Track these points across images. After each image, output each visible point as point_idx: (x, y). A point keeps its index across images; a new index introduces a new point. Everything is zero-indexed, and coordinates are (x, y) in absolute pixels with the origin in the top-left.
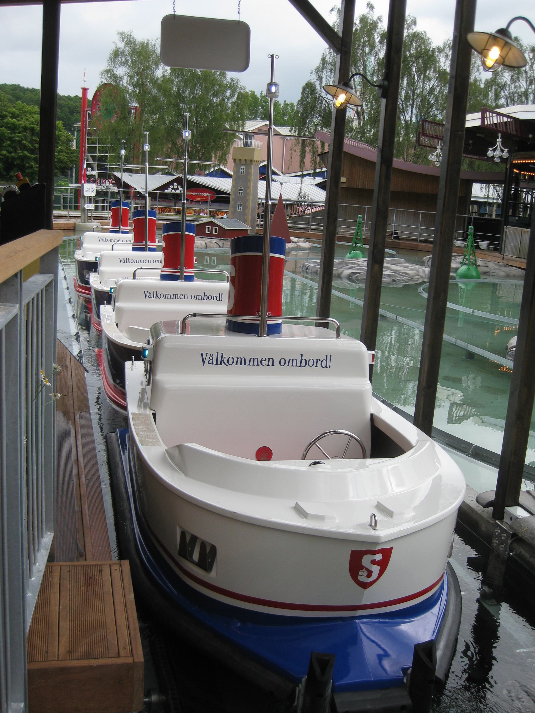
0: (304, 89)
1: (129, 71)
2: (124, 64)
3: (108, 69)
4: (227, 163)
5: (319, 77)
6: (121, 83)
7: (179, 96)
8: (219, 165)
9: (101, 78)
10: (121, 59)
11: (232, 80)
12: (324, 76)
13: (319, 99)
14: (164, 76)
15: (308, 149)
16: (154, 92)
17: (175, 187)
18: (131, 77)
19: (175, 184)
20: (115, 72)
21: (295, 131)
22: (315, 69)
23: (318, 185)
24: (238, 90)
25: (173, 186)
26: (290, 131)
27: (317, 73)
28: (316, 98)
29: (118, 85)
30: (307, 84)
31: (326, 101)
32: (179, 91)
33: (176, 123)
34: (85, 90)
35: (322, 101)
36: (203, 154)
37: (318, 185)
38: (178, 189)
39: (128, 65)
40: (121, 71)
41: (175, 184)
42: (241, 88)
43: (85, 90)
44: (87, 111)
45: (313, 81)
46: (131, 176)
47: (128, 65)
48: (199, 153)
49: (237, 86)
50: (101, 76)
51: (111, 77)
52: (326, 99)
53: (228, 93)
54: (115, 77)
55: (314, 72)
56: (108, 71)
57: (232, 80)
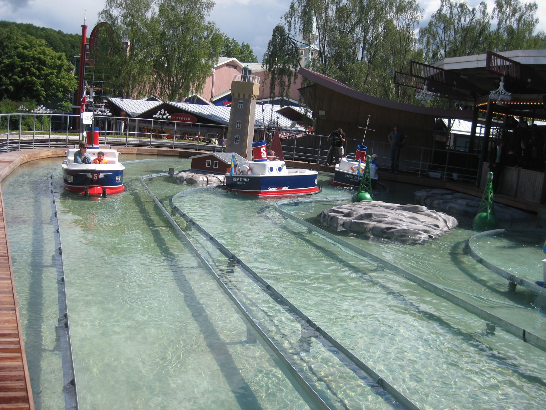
0: (275, 31)
1: (123, 13)
2: (119, 6)
3: (105, 10)
4: (202, 92)
5: (288, 21)
6: (116, 22)
7: (164, 34)
8: (196, 93)
9: (99, 17)
10: (117, 2)
11: (209, 23)
12: (293, 21)
13: (288, 40)
14: (152, 17)
15: (277, 82)
16: (144, 30)
17: (163, 112)
18: (125, 17)
19: (163, 110)
20: (111, 13)
21: (266, 67)
22: (285, 15)
23: (279, 112)
24: (214, 32)
25: (161, 111)
26: (263, 67)
27: (286, 18)
28: (285, 39)
29: (113, 23)
30: (276, 27)
31: (293, 42)
32: (164, 30)
33: (161, 57)
34: (84, 28)
35: (290, 42)
36: (183, 84)
37: (279, 112)
38: (164, 114)
39: (122, 7)
40: (116, 12)
41: (163, 110)
42: (216, 30)
43: (84, 28)
44: (86, 44)
45: (282, 24)
46: (123, 101)
47: (122, 7)
48: (179, 83)
49: (213, 28)
50: (99, 15)
51: (107, 17)
52: (293, 41)
53: (206, 33)
54: (111, 16)
55: (283, 17)
56: (104, 12)
57: (209, 23)
